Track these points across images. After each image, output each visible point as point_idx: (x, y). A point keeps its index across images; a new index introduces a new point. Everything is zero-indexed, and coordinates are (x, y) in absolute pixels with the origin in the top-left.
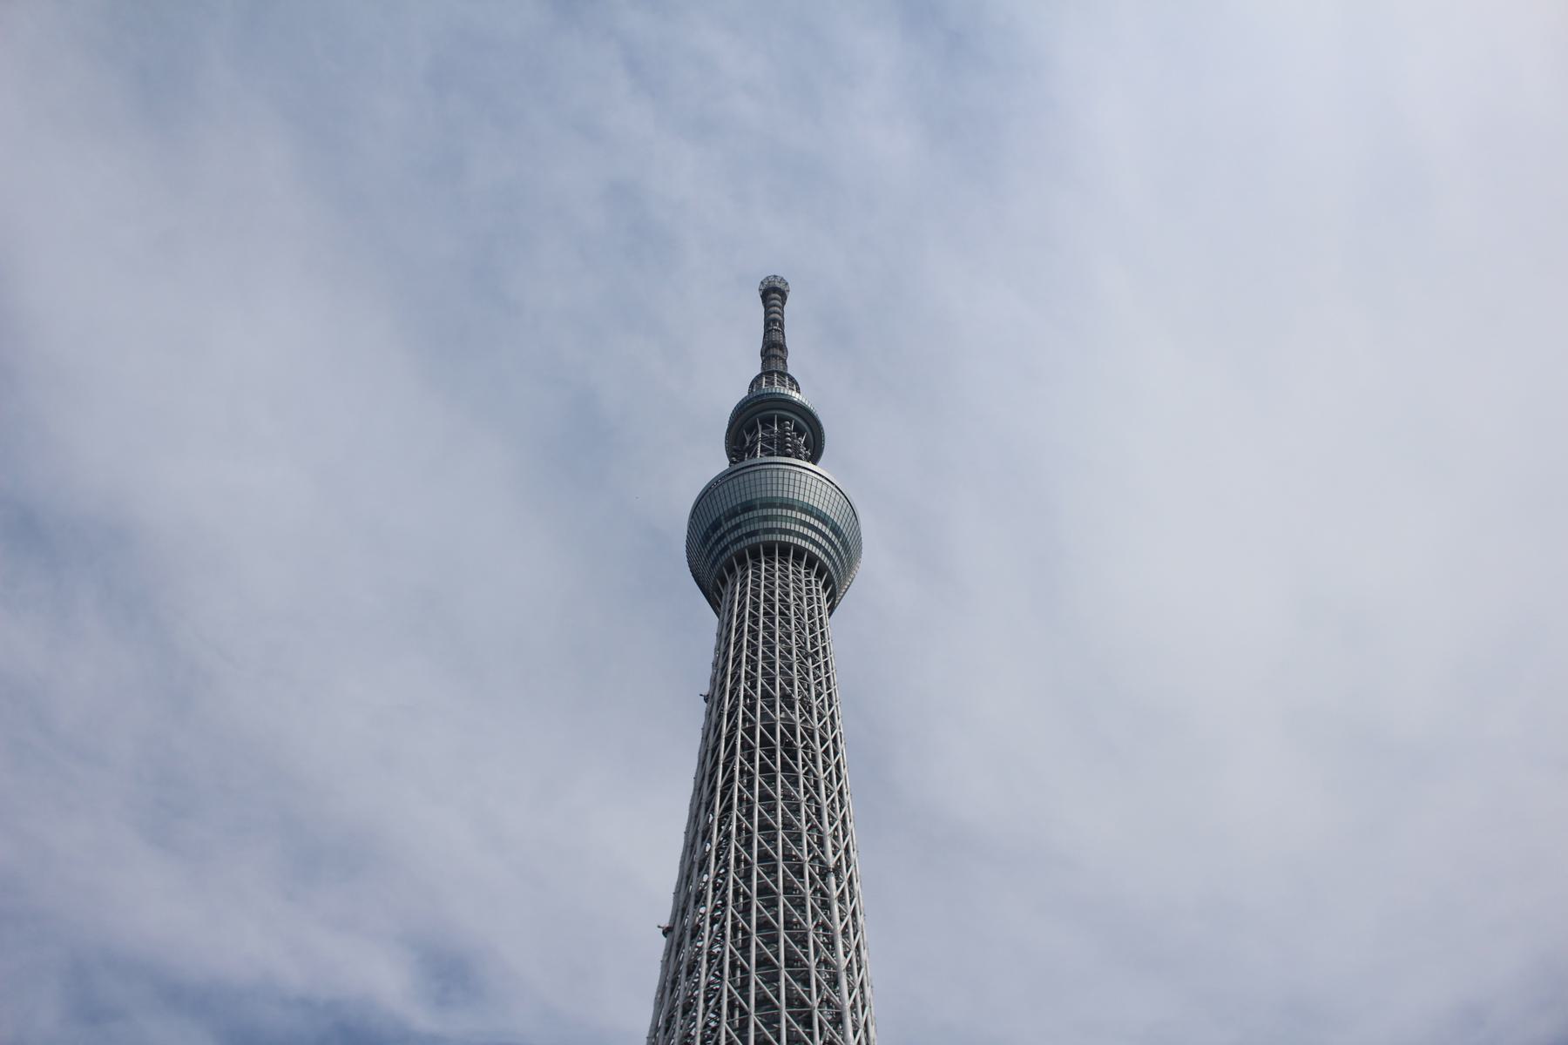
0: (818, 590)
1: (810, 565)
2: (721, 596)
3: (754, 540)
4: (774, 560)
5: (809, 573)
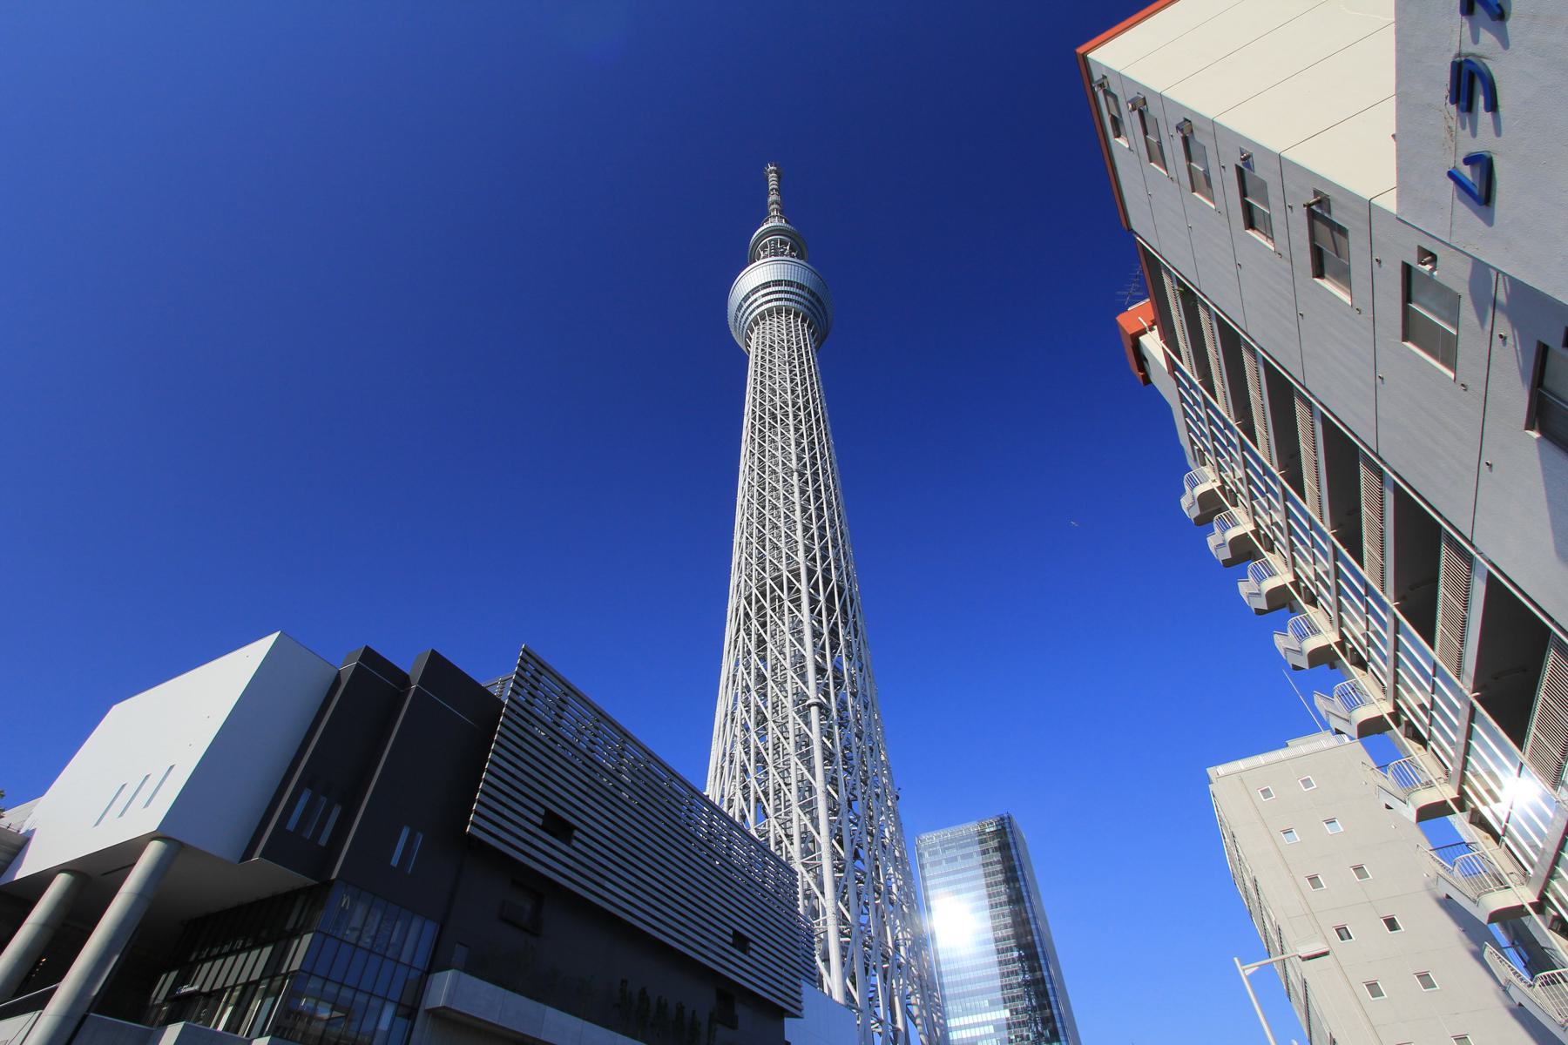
2: (750, 339)
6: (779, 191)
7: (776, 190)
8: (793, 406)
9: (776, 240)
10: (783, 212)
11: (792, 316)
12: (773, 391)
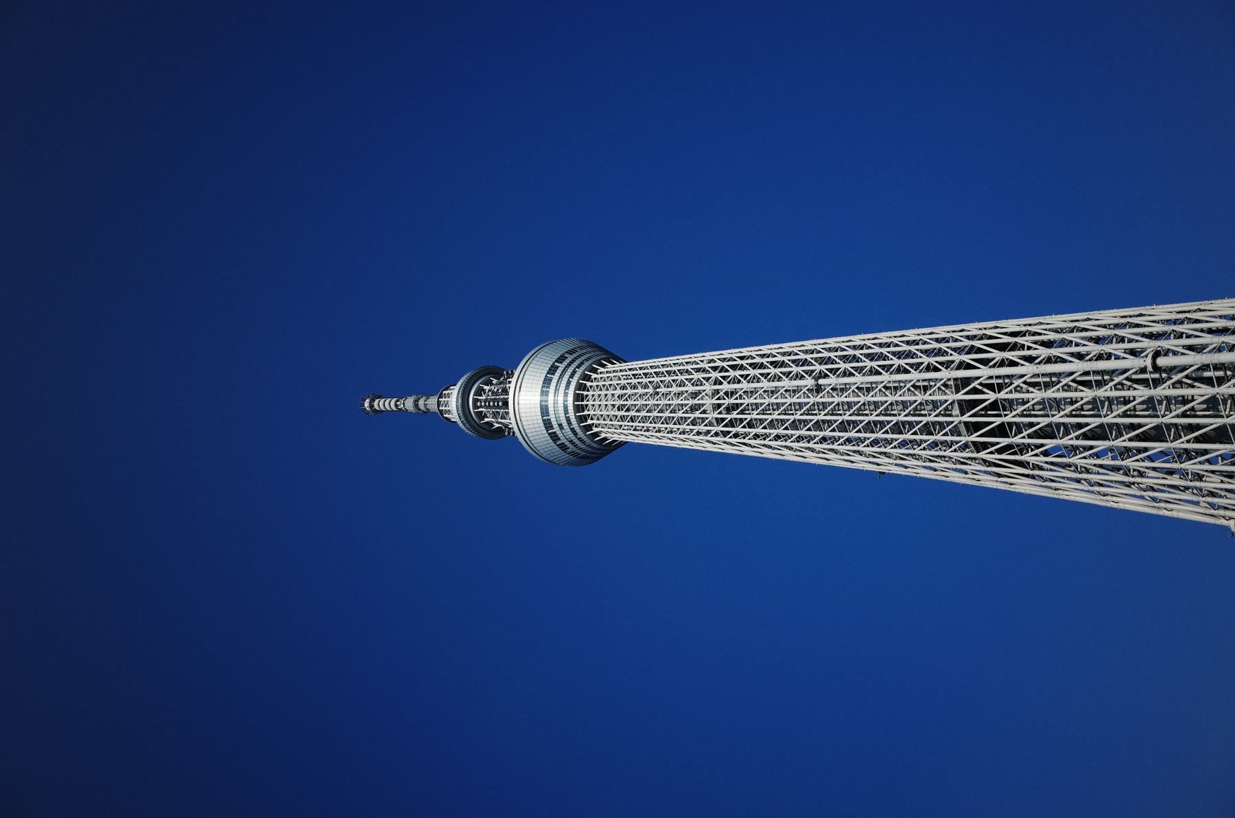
0: (607, 372)
1: (588, 378)
3: (573, 420)
4: (587, 405)
5: (595, 379)
6: (401, 396)
7: (397, 401)
8: (721, 383)
9: (475, 401)
10: (439, 389)
11: (589, 384)
12: (694, 409)
